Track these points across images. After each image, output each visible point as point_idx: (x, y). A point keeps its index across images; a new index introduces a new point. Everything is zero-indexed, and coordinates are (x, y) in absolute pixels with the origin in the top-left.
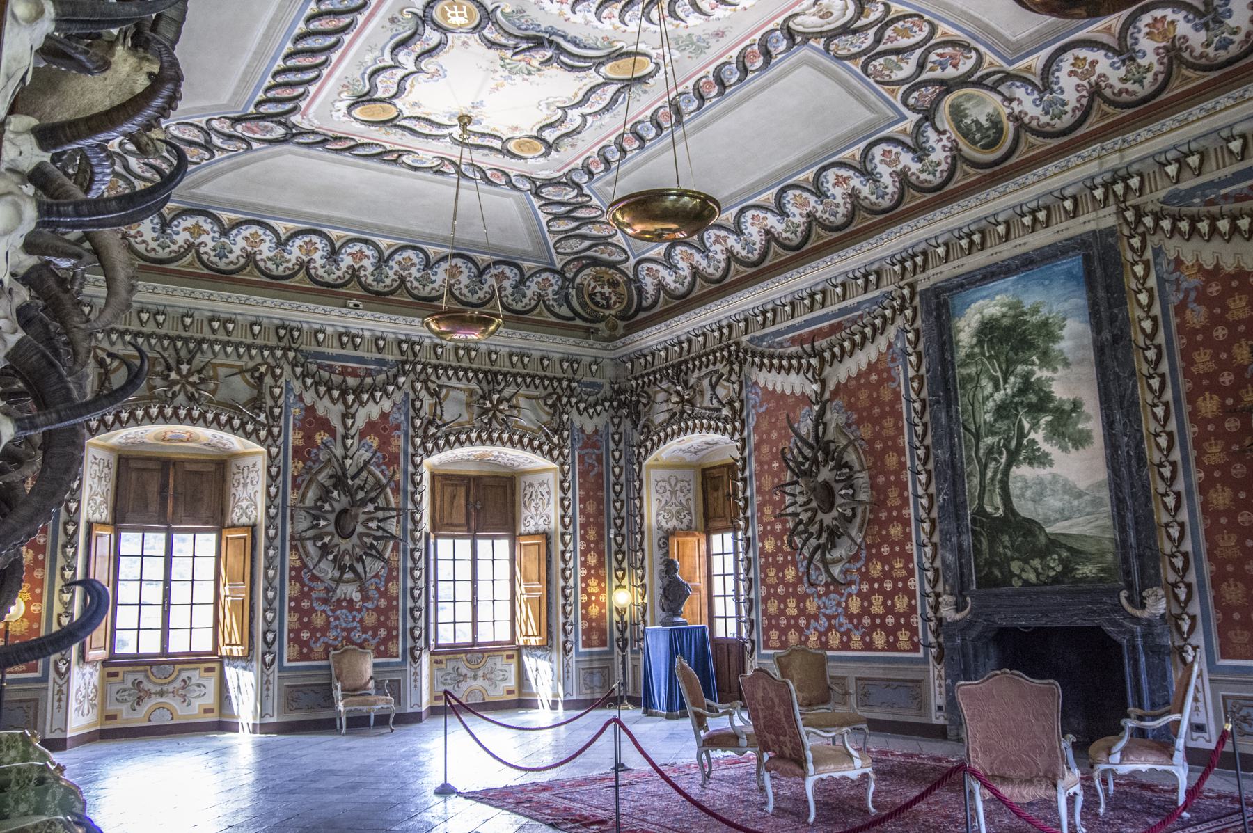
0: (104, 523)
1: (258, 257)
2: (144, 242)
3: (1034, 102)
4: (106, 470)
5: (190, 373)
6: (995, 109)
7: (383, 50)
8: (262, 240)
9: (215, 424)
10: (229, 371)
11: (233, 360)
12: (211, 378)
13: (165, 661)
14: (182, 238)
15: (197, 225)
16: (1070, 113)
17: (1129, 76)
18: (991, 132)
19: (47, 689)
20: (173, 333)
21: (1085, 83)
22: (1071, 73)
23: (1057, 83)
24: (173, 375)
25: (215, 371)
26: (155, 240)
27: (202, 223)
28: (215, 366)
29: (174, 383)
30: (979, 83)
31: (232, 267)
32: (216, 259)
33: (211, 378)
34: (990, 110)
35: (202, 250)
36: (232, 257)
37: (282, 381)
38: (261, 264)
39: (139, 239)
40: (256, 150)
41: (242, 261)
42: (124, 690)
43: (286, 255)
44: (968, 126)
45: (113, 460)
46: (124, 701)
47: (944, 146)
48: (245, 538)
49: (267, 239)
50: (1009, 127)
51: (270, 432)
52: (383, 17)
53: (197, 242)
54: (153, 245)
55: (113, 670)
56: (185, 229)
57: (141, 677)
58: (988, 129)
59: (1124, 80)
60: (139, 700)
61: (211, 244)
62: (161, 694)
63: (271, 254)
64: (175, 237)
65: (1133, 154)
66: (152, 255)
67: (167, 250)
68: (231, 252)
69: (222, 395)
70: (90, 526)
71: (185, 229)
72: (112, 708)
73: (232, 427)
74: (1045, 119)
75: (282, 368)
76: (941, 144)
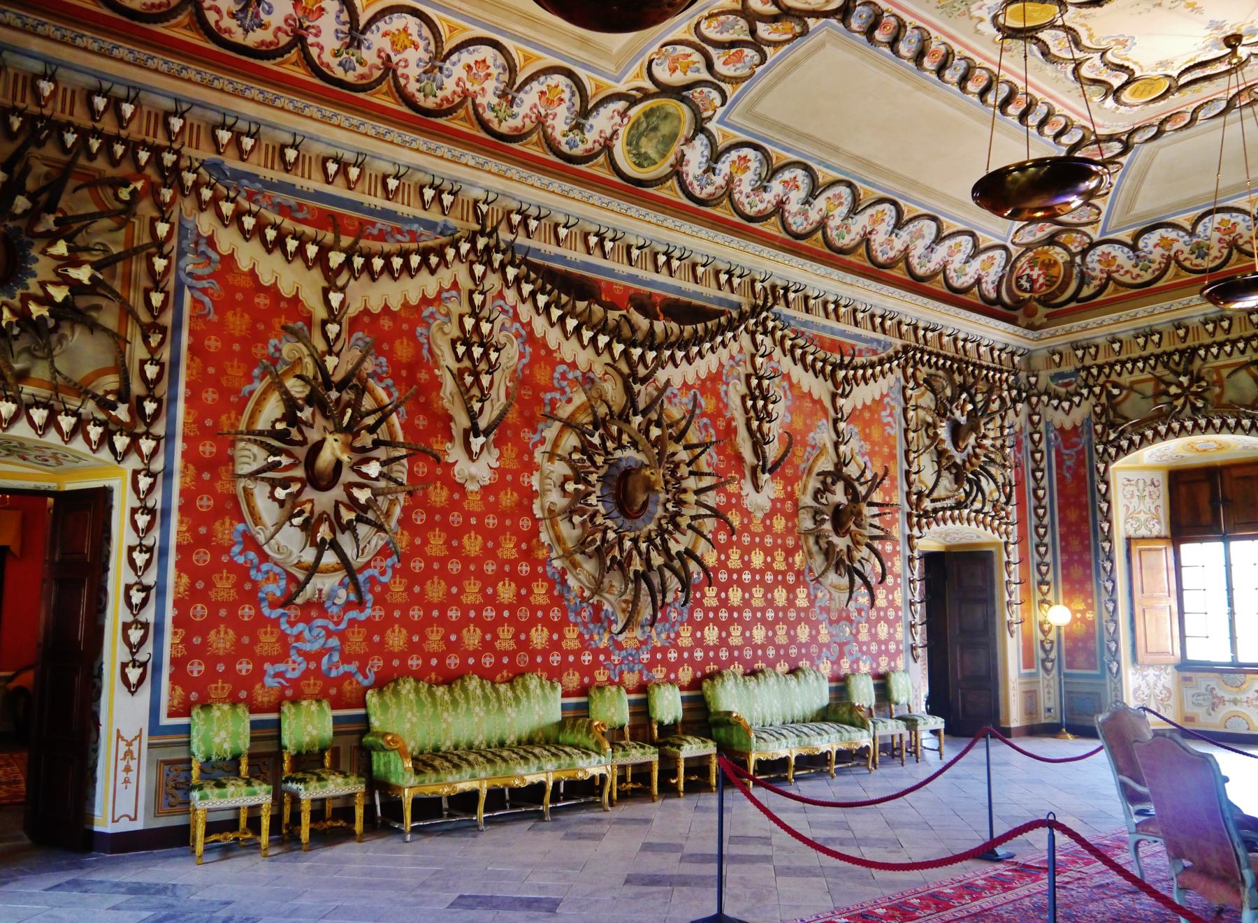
0: (1158, 538)
1: (1240, 242)
2: (1127, 272)
4: (1152, 488)
5: (1180, 385)
8: (1234, 224)
9: (1225, 429)
10: (1230, 370)
11: (1238, 358)
12: (1214, 384)
13: (1237, 669)
14: (1157, 254)
19: (1104, 685)
20: (1172, 348)
24: (1173, 390)
25: (1219, 374)
26: (1136, 266)
27: (1166, 235)
28: (1217, 369)
29: (1177, 396)
31: (1218, 262)
32: (1199, 261)
33: (1214, 384)
35: (1181, 258)
36: (1214, 252)
39: (1122, 272)
40: (1129, 163)
41: (1225, 252)
42: (1199, 695)
45: (1162, 479)
46: (1200, 705)
48: (1140, 551)
53: (1172, 253)
54: (1136, 271)
55: (1188, 674)
56: (1155, 246)
57: (1213, 684)
60: (1214, 707)
61: (1187, 249)
62: (1235, 702)
64: (1151, 257)
66: (1139, 281)
67: (1150, 271)
69: (1230, 395)
70: (1129, 540)
72: (1190, 710)
73: (1243, 427)
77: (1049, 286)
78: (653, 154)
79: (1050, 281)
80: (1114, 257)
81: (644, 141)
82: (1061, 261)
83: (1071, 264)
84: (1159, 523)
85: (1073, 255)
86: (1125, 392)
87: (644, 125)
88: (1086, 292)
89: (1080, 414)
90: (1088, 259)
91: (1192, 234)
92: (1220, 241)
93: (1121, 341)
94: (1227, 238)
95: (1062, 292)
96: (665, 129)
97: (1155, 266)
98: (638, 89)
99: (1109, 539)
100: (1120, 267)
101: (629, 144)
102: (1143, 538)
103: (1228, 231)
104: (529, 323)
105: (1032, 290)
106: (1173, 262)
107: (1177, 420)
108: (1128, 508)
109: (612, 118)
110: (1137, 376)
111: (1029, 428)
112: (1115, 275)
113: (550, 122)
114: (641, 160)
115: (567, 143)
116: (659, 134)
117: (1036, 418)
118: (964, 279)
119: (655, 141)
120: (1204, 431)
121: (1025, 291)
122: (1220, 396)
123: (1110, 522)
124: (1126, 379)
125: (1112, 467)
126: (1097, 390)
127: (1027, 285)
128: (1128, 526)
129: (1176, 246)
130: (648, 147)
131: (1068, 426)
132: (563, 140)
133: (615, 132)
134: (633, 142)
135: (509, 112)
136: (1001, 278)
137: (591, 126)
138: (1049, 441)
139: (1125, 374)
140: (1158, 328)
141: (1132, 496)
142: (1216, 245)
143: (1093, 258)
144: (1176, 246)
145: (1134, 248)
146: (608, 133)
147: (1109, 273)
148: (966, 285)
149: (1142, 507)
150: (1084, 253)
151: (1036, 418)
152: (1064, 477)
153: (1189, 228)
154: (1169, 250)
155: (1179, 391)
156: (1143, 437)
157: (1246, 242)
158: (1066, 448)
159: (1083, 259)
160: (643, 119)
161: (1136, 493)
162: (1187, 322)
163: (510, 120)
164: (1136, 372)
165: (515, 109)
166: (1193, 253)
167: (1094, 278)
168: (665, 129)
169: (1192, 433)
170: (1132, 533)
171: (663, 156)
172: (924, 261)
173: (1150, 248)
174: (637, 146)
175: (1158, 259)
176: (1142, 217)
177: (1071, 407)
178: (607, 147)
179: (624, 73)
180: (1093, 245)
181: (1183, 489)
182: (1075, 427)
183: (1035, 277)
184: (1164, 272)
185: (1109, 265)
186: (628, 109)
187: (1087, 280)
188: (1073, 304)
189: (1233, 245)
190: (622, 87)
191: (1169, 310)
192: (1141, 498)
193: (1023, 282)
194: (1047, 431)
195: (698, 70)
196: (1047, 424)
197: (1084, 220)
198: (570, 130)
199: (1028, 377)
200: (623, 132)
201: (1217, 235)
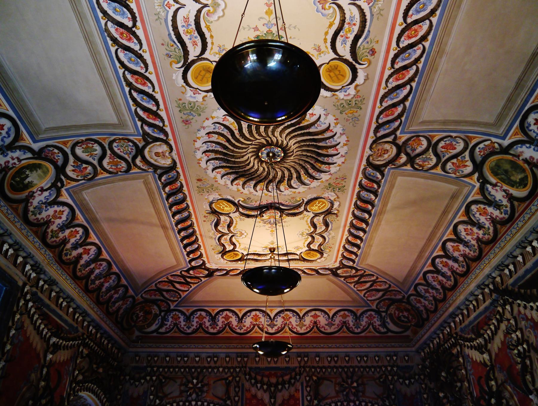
3: (41, 201)
6: (36, 185)
7: (372, 15)
16: (35, 218)
17: (54, 232)
18: (21, 185)
21: (51, 218)
22: (56, 211)
23: (51, 208)
30: (58, 179)
34: (35, 182)
44: (25, 173)
47: (8, 162)
50: (25, 194)
52: (380, 52)
58: (23, 183)
59: (52, 231)
65: (47, 269)
74: (31, 209)
76: (10, 160)
78: (520, 176)
81: (512, 178)
87: (503, 176)
96: (507, 167)
98: (478, 180)
101: (512, 186)
104: (532, 317)
109: (497, 190)
113: (494, 216)
114: (523, 183)
115: (505, 214)
116: (510, 170)
119: (514, 173)
130: (517, 177)
132: (503, 215)
133: (505, 191)
134: (512, 184)
135: (487, 229)
137: (500, 200)
146: (504, 193)
160: (499, 177)
163: (489, 231)
165: (486, 226)
168: (507, 167)
171: (524, 171)
174: (515, 182)
178: (511, 198)
179: (470, 184)
186: (491, 184)
190: (478, 185)
195: (464, 157)
198: (500, 210)
200: (505, 187)
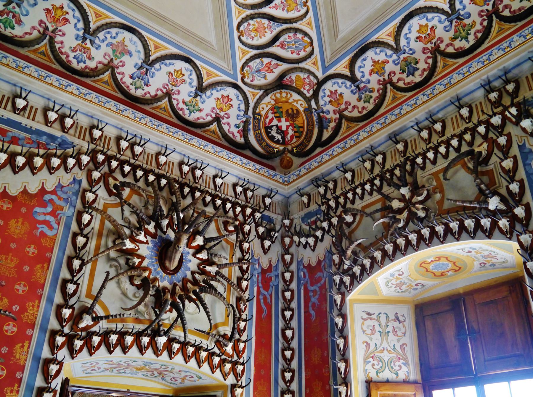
0: (405, 382)
1: (442, 47)
2: (354, 107)
4: (396, 324)
15: (375, 62)
26: (359, 100)
27: (376, 58)
32: (411, 78)
35: (395, 80)
37: (515, 150)
38: (450, 50)
39: (350, 108)
43: (467, 21)
49: (435, 22)
51: (514, 219)
53: (386, 77)
54: (361, 104)
61: (397, 69)
63: (452, 33)
64: (369, 86)
66: (365, 112)
67: (372, 100)
68: (417, 62)
70: (369, 383)
71: (370, 74)
75: (509, 135)
77: (299, 137)
79: (298, 133)
80: (341, 95)
82: (301, 109)
83: (309, 110)
84: (406, 364)
85: (308, 100)
86: (358, 218)
88: (326, 135)
89: (322, 248)
90: (321, 102)
91: (397, 50)
92: (424, 50)
93: (353, 171)
94: (429, 46)
95: (309, 141)
97: (375, 95)
99: (346, 382)
100: (348, 103)
102: (388, 381)
103: (429, 38)
105: (284, 143)
106: (388, 86)
107: (401, 235)
108: (368, 345)
110: (368, 199)
111: (281, 268)
112: (346, 113)
117: (288, 257)
118: (197, 115)
120: (429, 242)
121: (278, 142)
122: (441, 202)
123: (347, 361)
124: (359, 204)
125: (350, 297)
126: (335, 221)
127: (279, 137)
128: (369, 367)
129: (389, 67)
131: (314, 263)
136: (246, 123)
138: (299, 279)
139: (358, 201)
140: (381, 149)
141: (373, 331)
142: (421, 57)
143: (324, 100)
144: (389, 67)
145: (353, 79)
147: (340, 112)
148: (201, 121)
149: (385, 345)
150: (315, 95)
151: (288, 257)
152: (310, 315)
153: (393, 43)
154: (383, 74)
155: (402, 205)
156: (373, 259)
157: (447, 46)
158: (312, 285)
159: (317, 103)
161: (378, 328)
162: (404, 135)
164: (367, 197)
166: (404, 72)
167: (330, 121)
169: (417, 248)
170: (373, 375)
172: (139, 83)
173: (367, 76)
175: (376, 87)
176: (348, 42)
177: (316, 243)
180: (321, 84)
181: (429, 324)
182: (319, 262)
183: (284, 129)
184: (382, 97)
185: (339, 104)
187: (325, 124)
188: (319, 150)
189: (436, 51)
191: (385, 126)
192: (384, 334)
193: (274, 133)
194: (298, 269)
196: (299, 263)
197: (302, 54)
199: (283, 220)
201: (418, 46)
